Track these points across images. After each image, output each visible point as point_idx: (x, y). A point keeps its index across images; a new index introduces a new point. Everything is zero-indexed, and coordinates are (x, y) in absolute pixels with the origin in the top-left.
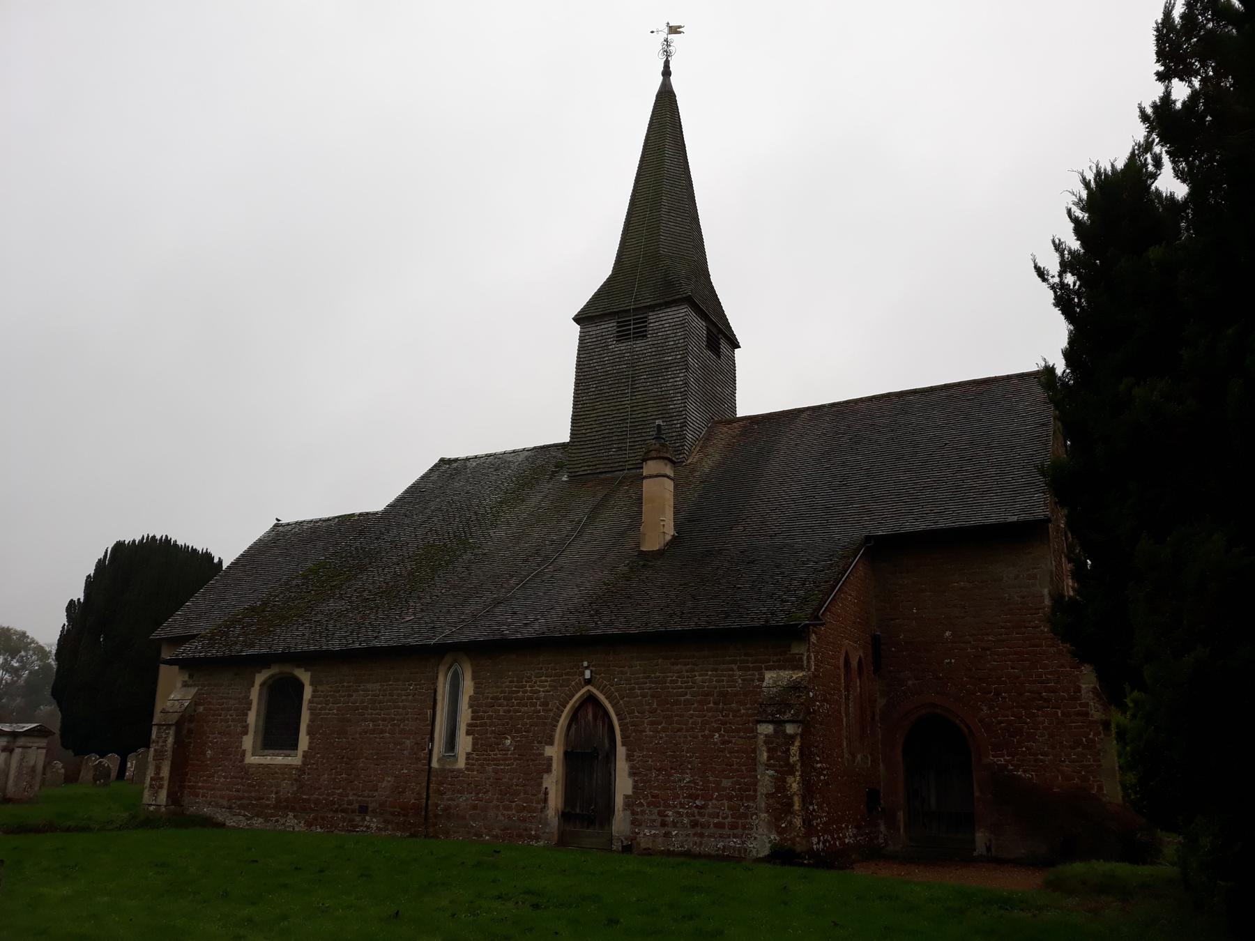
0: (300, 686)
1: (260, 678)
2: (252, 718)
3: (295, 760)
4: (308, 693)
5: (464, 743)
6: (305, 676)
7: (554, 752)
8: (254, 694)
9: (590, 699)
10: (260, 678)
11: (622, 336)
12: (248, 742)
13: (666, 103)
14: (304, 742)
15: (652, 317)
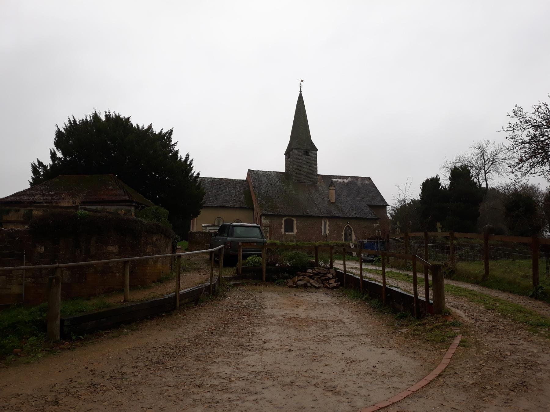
0: (293, 221)
1: (284, 219)
2: (283, 226)
3: (295, 234)
4: (295, 222)
5: (328, 232)
6: (294, 219)
7: (343, 233)
8: (283, 222)
9: (348, 226)
10: (284, 219)
11: (303, 154)
12: (283, 230)
13: (301, 98)
14: (295, 230)
15: (309, 152)
